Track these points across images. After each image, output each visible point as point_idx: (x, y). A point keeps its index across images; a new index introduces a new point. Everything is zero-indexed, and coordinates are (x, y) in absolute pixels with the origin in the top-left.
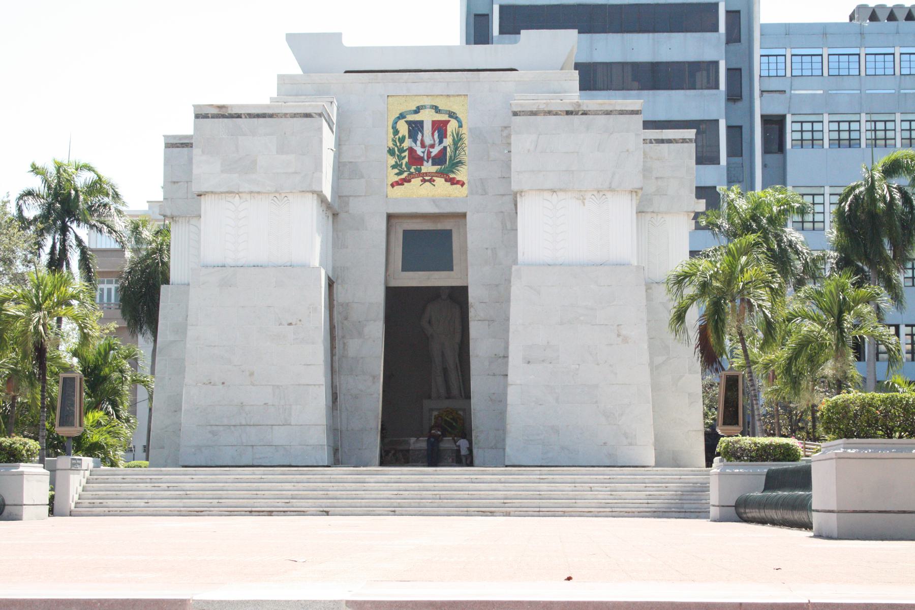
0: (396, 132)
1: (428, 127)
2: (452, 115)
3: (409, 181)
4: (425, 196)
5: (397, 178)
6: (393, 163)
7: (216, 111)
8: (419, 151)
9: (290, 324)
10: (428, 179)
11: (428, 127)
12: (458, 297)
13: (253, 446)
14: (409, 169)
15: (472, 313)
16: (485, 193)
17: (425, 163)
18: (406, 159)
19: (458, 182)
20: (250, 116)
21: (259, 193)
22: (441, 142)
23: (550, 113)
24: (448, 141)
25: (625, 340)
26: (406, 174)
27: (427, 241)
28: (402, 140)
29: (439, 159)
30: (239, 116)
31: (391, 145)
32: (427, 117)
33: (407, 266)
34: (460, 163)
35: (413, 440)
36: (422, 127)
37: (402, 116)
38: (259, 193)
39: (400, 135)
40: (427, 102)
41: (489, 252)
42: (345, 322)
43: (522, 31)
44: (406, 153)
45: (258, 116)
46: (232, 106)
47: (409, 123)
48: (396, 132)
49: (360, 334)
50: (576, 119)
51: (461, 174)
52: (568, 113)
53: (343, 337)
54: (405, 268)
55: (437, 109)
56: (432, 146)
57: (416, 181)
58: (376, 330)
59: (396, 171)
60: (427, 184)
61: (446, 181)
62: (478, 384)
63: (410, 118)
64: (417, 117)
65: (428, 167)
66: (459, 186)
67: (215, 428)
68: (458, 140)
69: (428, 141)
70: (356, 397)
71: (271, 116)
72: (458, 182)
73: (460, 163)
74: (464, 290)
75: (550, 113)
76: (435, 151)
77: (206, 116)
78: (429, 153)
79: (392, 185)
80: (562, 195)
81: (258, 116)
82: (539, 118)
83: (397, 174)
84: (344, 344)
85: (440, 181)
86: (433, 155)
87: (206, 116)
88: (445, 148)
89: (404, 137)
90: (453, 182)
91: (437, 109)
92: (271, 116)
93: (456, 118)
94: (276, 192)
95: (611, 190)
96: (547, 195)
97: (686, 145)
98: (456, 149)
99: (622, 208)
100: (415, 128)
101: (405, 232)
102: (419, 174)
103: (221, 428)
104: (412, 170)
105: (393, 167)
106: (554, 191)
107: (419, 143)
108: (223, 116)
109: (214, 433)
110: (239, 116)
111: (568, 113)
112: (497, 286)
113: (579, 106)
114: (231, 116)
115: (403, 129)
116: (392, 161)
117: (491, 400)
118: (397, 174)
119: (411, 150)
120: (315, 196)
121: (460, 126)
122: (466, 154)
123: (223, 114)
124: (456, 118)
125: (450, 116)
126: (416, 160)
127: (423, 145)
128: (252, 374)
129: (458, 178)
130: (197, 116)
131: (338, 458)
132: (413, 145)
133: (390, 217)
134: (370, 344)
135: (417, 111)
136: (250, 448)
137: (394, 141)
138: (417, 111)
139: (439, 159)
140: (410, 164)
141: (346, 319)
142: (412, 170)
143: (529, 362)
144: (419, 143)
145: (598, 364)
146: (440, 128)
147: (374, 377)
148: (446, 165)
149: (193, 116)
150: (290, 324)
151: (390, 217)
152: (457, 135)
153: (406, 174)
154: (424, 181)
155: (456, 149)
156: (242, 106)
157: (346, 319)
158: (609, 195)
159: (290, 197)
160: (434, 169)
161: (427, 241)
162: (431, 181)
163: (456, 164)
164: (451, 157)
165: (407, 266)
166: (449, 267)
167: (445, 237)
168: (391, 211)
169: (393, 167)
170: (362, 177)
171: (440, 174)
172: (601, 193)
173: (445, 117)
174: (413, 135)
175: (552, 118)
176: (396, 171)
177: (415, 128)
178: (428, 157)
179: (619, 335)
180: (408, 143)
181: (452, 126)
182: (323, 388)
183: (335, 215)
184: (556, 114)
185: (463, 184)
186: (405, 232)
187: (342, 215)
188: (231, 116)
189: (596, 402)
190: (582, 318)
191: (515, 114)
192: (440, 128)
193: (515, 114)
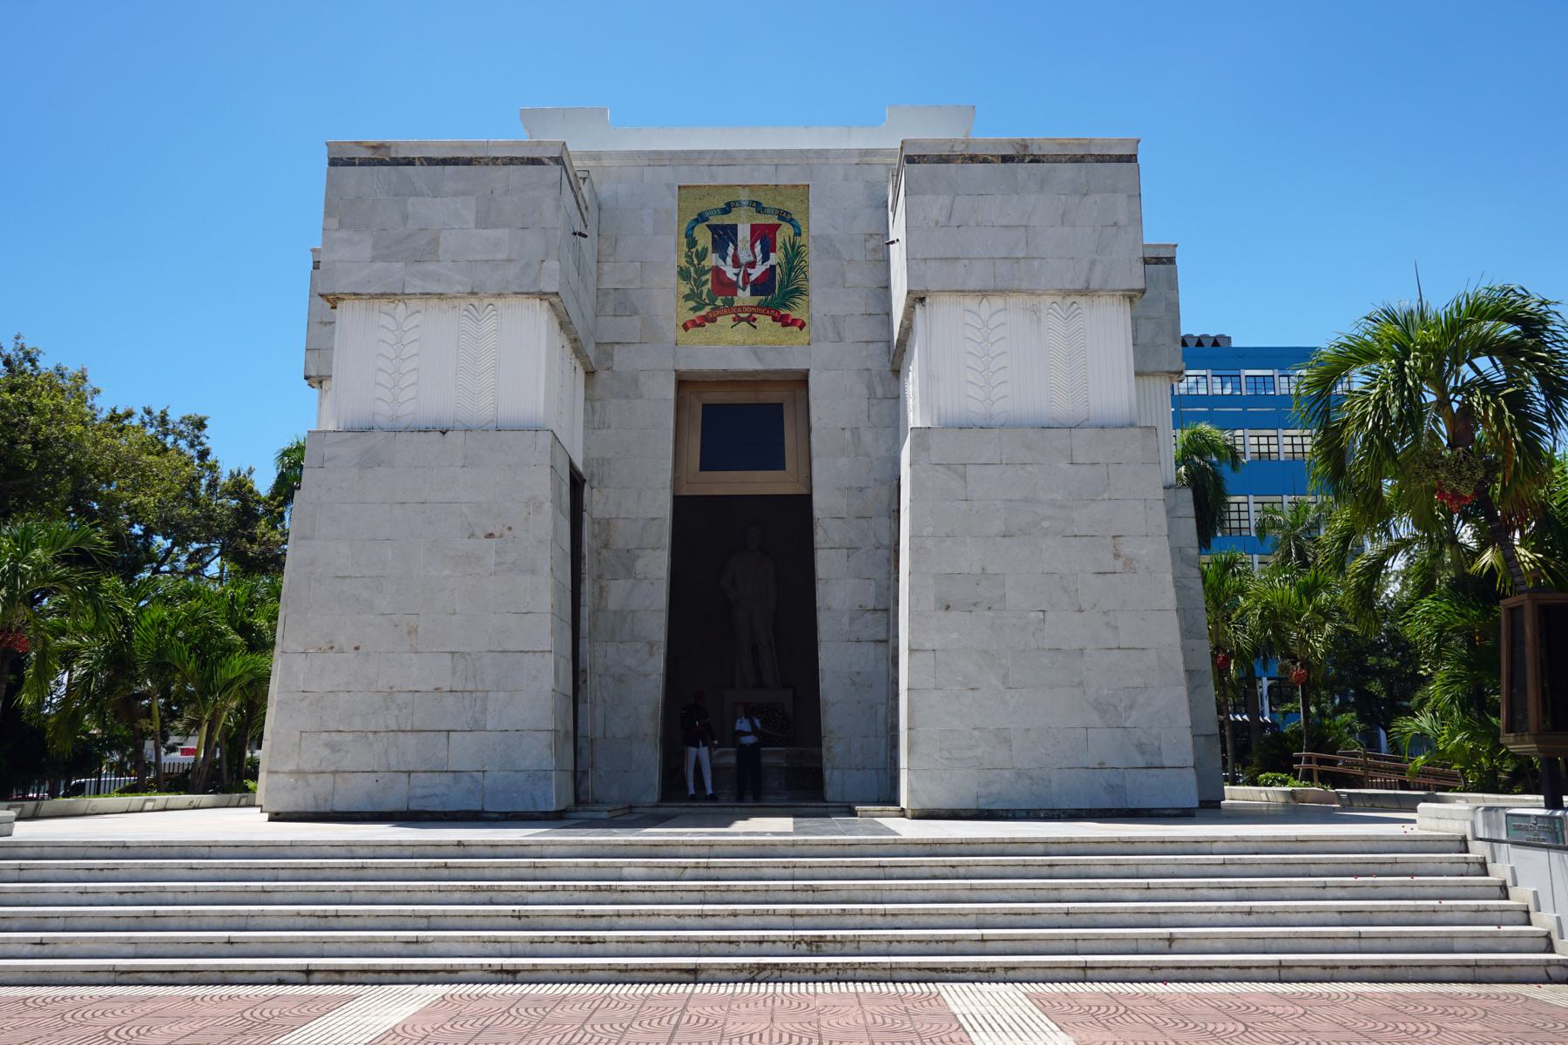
0: (692, 242)
1: (744, 232)
2: (784, 216)
3: (714, 320)
5: (693, 316)
6: (687, 291)
7: (367, 154)
8: (730, 272)
9: (491, 535)
11: (744, 232)
13: (409, 772)
14: (713, 302)
15: (819, 536)
16: (841, 340)
17: (740, 292)
18: (709, 285)
19: (794, 322)
20: (431, 162)
21: (440, 296)
22: (765, 258)
23: (973, 159)
25: (1130, 564)
26: (708, 309)
28: (702, 256)
29: (762, 286)
30: (410, 162)
31: (683, 263)
34: (799, 292)
36: (736, 235)
37: (701, 218)
38: (440, 296)
39: (699, 247)
41: (848, 434)
42: (604, 552)
44: (709, 276)
45: (444, 162)
46: (398, 144)
47: (713, 228)
48: (692, 242)
49: (629, 572)
50: (1022, 169)
52: (1006, 159)
53: (600, 577)
54: (705, 466)
55: (758, 207)
56: (752, 265)
57: (726, 320)
58: (657, 564)
59: (692, 304)
60: (744, 325)
61: (774, 319)
62: (836, 657)
63: (715, 220)
64: (727, 220)
65: (744, 297)
66: (795, 329)
67: (336, 737)
68: (795, 254)
69: (745, 257)
70: (620, 680)
71: (469, 162)
72: (794, 322)
74: (801, 506)
75: (973, 159)
76: (755, 273)
77: (350, 162)
78: (747, 275)
79: (686, 327)
80: (998, 302)
81: (444, 162)
82: (952, 167)
83: (694, 309)
84: (601, 588)
85: (764, 320)
86: (752, 278)
87: (350, 162)
88: (773, 268)
89: (705, 250)
90: (785, 322)
91: (758, 207)
92: (469, 162)
93: (791, 221)
94: (473, 293)
95: (1085, 292)
96: (971, 302)
97: (1162, 267)
98: (791, 270)
101: (707, 408)
102: (730, 307)
103: (350, 737)
104: (719, 302)
105: (687, 298)
106: (984, 293)
107: (729, 260)
108: (382, 163)
109: (334, 748)
110: (410, 162)
111: (1006, 159)
112: (861, 490)
113: (1026, 147)
114: (396, 162)
115: (704, 238)
116: (686, 289)
117: (854, 683)
118: (694, 309)
119: (717, 272)
120: (546, 304)
121: (798, 234)
123: (381, 158)
124: (791, 221)
125: (781, 218)
126: (724, 286)
127: (736, 263)
129: (794, 315)
130: (333, 162)
132: (721, 262)
134: (644, 590)
135: (727, 209)
136: (404, 777)
137: (688, 256)
138: (727, 209)
139: (762, 286)
141: (606, 546)
142: (719, 302)
143: (948, 608)
144: (729, 260)
145: (1081, 611)
147: (651, 645)
149: (326, 161)
150: (491, 535)
152: (793, 247)
153: (708, 309)
154: (738, 320)
155: (791, 270)
156: (418, 145)
157: (606, 546)
158: (1082, 301)
159: (499, 303)
160: (756, 300)
161: (743, 423)
162: (751, 320)
163: (794, 292)
164: (782, 282)
166: (777, 463)
167: (774, 413)
169: (687, 298)
170: (635, 312)
171: (764, 308)
172: (1069, 300)
173: (774, 220)
175: (978, 168)
176: (692, 304)
177: (724, 236)
178: (745, 283)
179: (1117, 556)
180: (712, 260)
181: (784, 233)
182: (551, 658)
183: (590, 374)
184: (985, 161)
185: (802, 326)
186: (706, 407)
187: (602, 375)
188: (396, 162)
189: (1081, 684)
190: (1045, 524)
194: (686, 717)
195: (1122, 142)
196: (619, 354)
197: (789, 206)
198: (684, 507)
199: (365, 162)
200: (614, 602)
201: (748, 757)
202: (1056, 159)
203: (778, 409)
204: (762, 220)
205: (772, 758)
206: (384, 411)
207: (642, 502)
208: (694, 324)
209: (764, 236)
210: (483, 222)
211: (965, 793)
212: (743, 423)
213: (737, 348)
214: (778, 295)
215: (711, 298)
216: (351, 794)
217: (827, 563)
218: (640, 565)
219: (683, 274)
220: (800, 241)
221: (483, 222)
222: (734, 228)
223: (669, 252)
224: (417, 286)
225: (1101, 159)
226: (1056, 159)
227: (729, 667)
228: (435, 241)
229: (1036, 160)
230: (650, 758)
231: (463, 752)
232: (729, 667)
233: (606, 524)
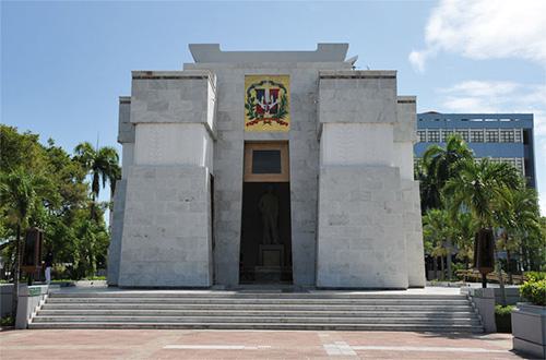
0: (250, 95)
1: (267, 92)
2: (281, 86)
8: (263, 106)
11: (267, 92)
12: (284, 189)
16: (300, 129)
20: (165, 78)
23: (342, 77)
24: (278, 101)
28: (253, 100)
29: (273, 111)
30: (158, 78)
32: (267, 88)
34: (286, 113)
35: (257, 267)
37: (253, 87)
40: (267, 79)
41: (302, 163)
43: (315, 48)
48: (250, 95)
51: (286, 119)
52: (353, 77)
55: (272, 83)
57: (261, 123)
58: (238, 206)
62: (297, 238)
63: (258, 88)
64: (262, 87)
65: (267, 115)
68: (284, 99)
69: (267, 101)
70: (226, 244)
71: (177, 78)
73: (286, 113)
75: (342, 77)
76: (271, 106)
77: (139, 78)
82: (336, 80)
85: (274, 122)
90: (282, 123)
91: (272, 83)
92: (177, 78)
96: (341, 125)
100: (260, 93)
110: (158, 78)
111: (353, 77)
114: (154, 78)
115: (254, 94)
116: (247, 111)
122: (289, 108)
123: (149, 76)
126: (261, 111)
127: (265, 103)
128: (163, 230)
130: (134, 78)
131: (215, 284)
133: (246, 143)
134: (234, 214)
135: (262, 83)
138: (262, 83)
139: (273, 111)
140: (256, 114)
146: (274, 93)
147: (237, 233)
148: (278, 114)
151: (246, 143)
160: (270, 116)
161: (266, 156)
162: (269, 123)
168: (248, 139)
171: (273, 119)
174: (259, 97)
177: (260, 93)
180: (256, 101)
181: (281, 92)
183: (215, 141)
187: (219, 141)
191: (322, 78)
193: (322, 78)
195: (391, 72)
196: (224, 134)
197: (283, 82)
198: (246, 185)
199: (144, 78)
200: (224, 218)
202: (370, 77)
203: (279, 152)
204: (273, 87)
207: (234, 186)
208: (252, 124)
209: (274, 93)
210: (183, 98)
212: (266, 156)
213: (265, 131)
215: (256, 114)
218: (232, 206)
219: (246, 106)
220: (287, 95)
221: (183, 98)
222: (264, 90)
223: (243, 100)
224: (163, 120)
225: (385, 77)
226: (370, 77)
227: (265, 242)
228: (168, 104)
229: (363, 78)
230: (235, 270)
232: (265, 242)
233: (220, 192)
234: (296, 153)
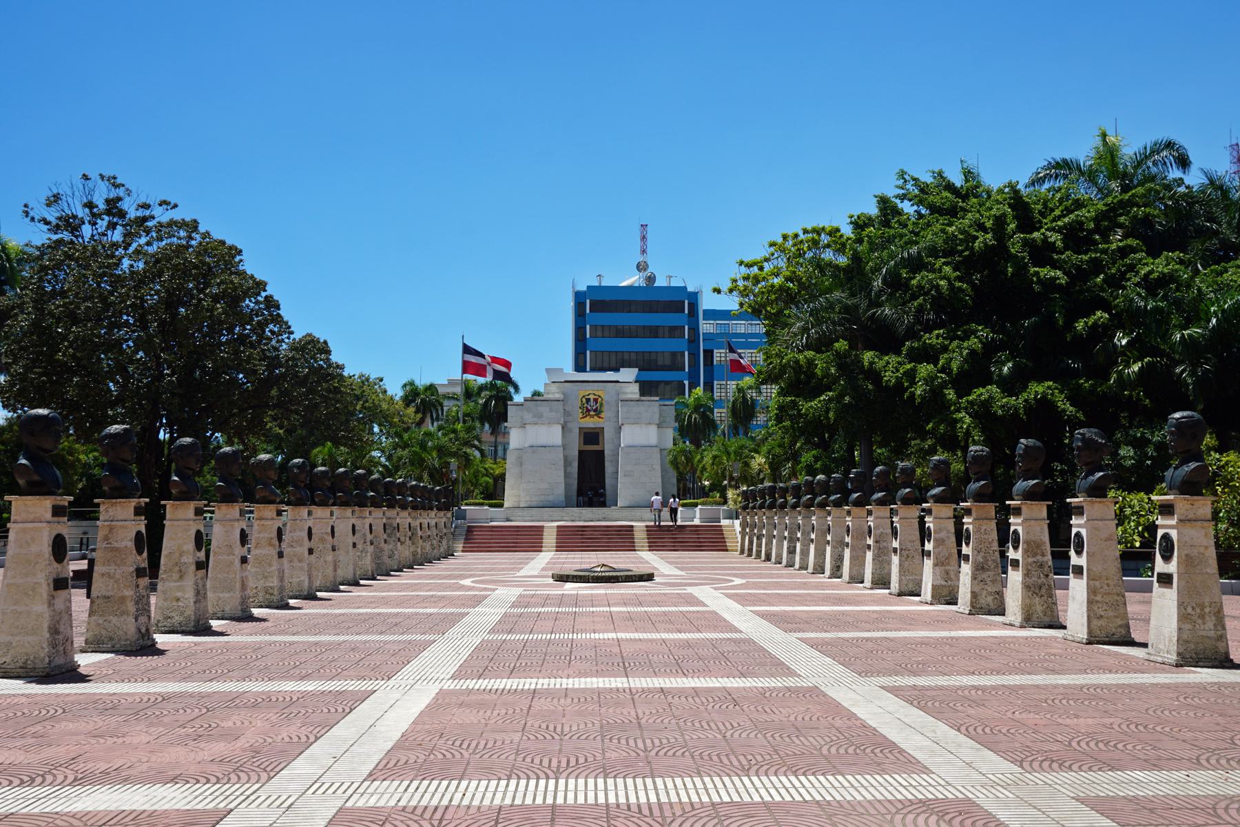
4: (591, 422)
10: (592, 417)
12: (601, 454)
27: (591, 437)
29: (595, 410)
32: (592, 397)
33: (585, 443)
51: (602, 415)
58: (576, 464)
62: (608, 481)
74: (602, 452)
99: (653, 430)
126: (588, 410)
131: (568, 505)
139: (595, 410)
140: (586, 412)
146: (596, 400)
148: (598, 412)
161: (591, 437)
165: (585, 443)
166: (598, 444)
167: (597, 434)
177: (588, 400)
192: (596, 400)
194: (580, 492)
198: (581, 452)
201: (590, 499)
205: (595, 499)
206: (535, 443)
207: (575, 453)
211: (627, 504)
214: (598, 412)
216: (534, 504)
217: (607, 464)
230: (575, 498)
231: (551, 498)
234: (608, 435)
